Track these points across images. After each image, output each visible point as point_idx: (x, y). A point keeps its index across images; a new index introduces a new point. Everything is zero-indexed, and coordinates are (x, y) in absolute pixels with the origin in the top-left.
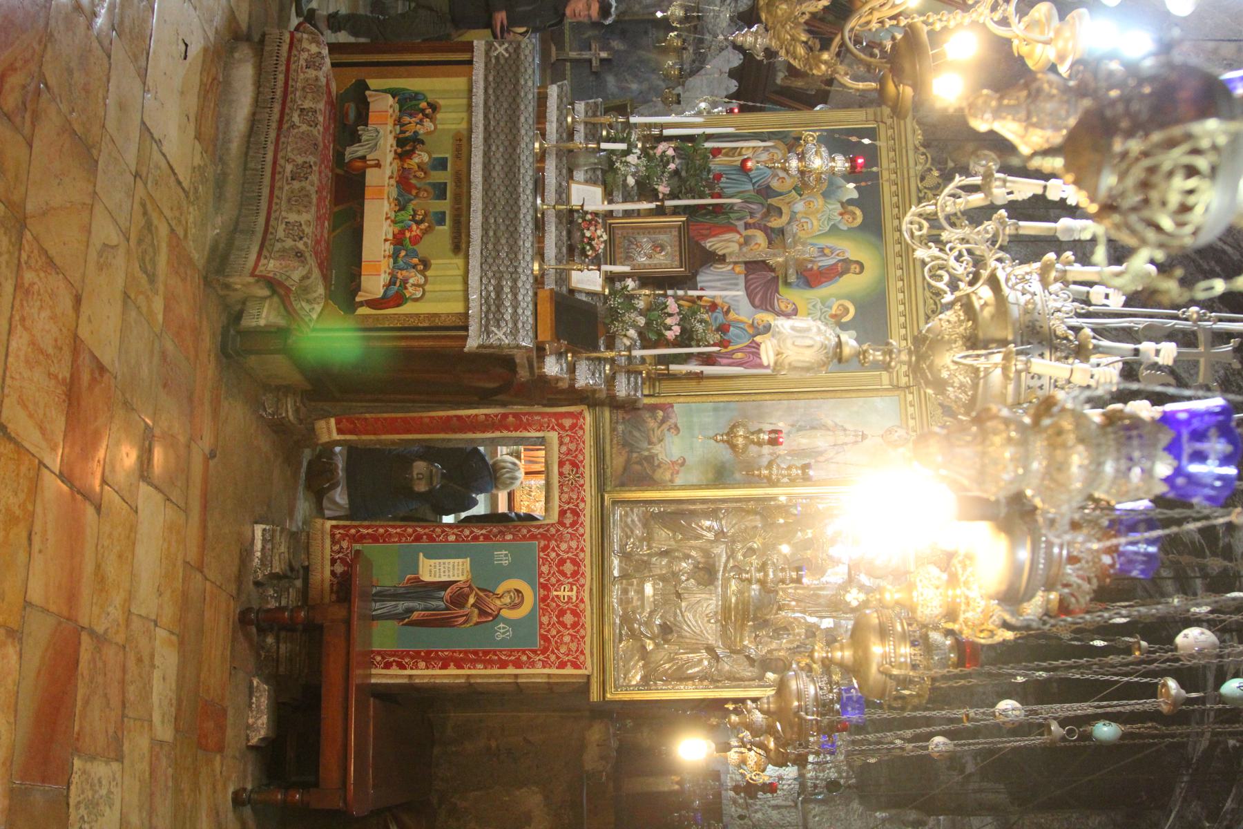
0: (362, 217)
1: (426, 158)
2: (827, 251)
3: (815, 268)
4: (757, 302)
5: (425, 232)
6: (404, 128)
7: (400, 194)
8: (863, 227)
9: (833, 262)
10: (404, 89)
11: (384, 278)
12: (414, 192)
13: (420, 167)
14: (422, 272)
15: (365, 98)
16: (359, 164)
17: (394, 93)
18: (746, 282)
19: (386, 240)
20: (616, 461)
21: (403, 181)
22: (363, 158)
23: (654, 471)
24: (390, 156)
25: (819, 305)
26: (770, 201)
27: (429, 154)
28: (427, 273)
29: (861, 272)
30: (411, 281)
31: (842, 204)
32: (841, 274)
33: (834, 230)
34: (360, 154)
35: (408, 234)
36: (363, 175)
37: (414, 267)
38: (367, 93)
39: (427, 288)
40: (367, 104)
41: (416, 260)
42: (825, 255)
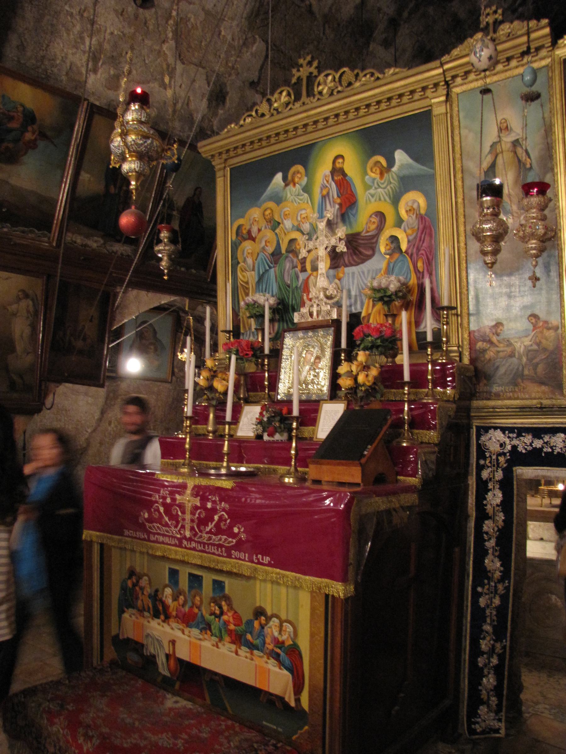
0: (216, 674)
1: (168, 591)
2: (325, 192)
3: (339, 201)
4: (369, 253)
5: (230, 605)
6: (146, 607)
7: (197, 627)
8: (305, 165)
9: (333, 185)
10: (119, 600)
11: (272, 665)
12: (196, 610)
13: (175, 599)
14: (268, 619)
15: (124, 639)
16: (172, 662)
17: (121, 612)
18: (352, 265)
19: (237, 653)
20: (535, 394)
21: (188, 620)
22: (168, 656)
23: (545, 349)
24: (167, 628)
25: (372, 191)
26: (283, 251)
27: (166, 586)
28: (269, 613)
29: (342, 157)
30: (276, 634)
31: (286, 185)
32: (344, 175)
33: (307, 189)
34: (164, 660)
35: (232, 627)
36: (180, 661)
37: (262, 627)
38: (121, 637)
39: (283, 617)
40: (128, 640)
41: (256, 624)
42: (328, 194)
